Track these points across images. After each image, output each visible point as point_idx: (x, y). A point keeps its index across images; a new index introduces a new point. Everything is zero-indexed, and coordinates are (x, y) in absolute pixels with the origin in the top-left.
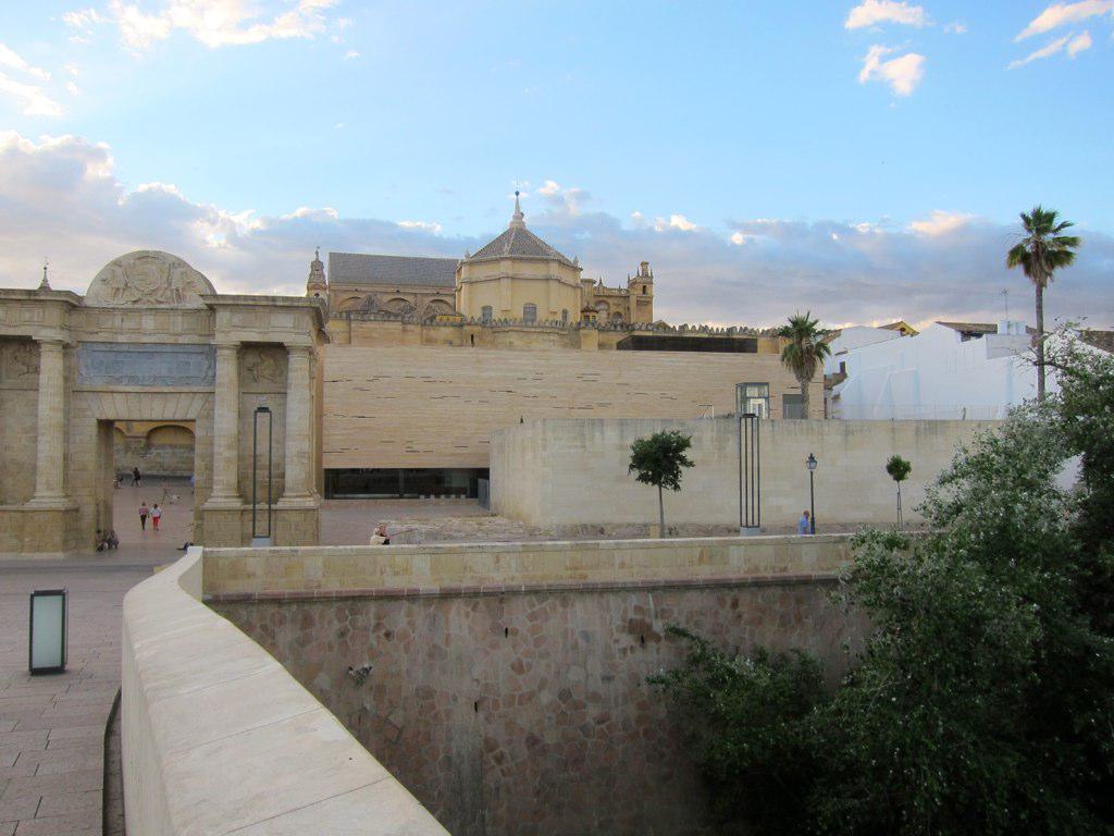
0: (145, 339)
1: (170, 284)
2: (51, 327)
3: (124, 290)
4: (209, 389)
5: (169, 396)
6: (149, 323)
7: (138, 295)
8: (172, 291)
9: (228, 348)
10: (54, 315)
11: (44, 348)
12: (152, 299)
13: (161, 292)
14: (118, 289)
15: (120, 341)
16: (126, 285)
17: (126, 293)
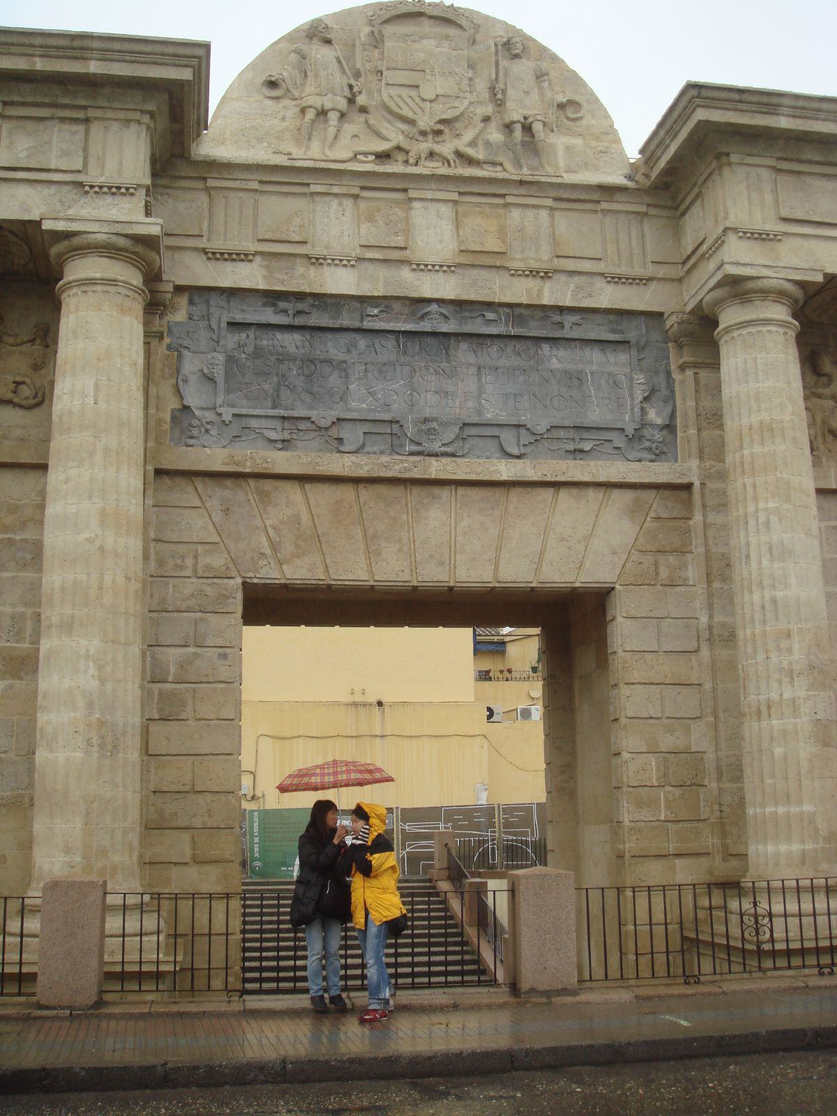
0: (428, 286)
1: (500, 104)
2: (115, 190)
3: (343, 115)
4: (661, 472)
5: (514, 493)
6: (434, 230)
7: (394, 135)
8: (508, 127)
9: (779, 295)
10: (125, 151)
11: (77, 270)
12: (446, 149)
13: (468, 136)
14: (322, 113)
15: (331, 289)
16: (351, 101)
17: (349, 128)
